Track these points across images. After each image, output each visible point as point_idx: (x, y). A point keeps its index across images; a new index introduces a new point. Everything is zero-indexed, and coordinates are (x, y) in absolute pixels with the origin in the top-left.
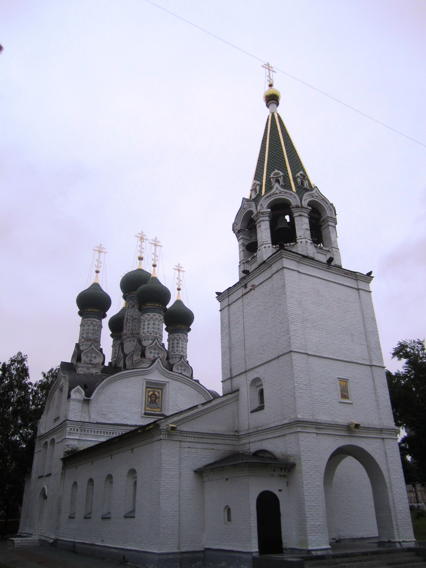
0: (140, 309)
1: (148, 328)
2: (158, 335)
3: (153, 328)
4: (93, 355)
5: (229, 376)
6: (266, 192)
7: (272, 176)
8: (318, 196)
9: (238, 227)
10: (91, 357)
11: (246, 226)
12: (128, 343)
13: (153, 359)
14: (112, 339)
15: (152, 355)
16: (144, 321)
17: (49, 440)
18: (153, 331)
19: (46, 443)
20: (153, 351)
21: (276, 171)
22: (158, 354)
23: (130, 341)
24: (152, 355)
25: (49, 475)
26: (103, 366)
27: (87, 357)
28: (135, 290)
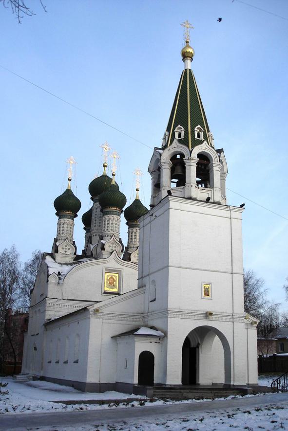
0: (102, 211)
1: (108, 227)
2: (115, 232)
3: (112, 227)
4: (67, 247)
5: (141, 276)
6: (170, 145)
7: (176, 129)
8: (206, 147)
9: (151, 169)
10: (66, 249)
11: (156, 171)
12: (95, 236)
13: (111, 251)
14: (85, 231)
15: (111, 248)
16: (105, 221)
17: (37, 310)
18: (112, 230)
19: (36, 311)
20: (111, 245)
21: (179, 126)
22: (115, 247)
23: (96, 235)
24: (111, 248)
25: (38, 334)
26: (75, 256)
27: (63, 248)
28: (99, 194)
